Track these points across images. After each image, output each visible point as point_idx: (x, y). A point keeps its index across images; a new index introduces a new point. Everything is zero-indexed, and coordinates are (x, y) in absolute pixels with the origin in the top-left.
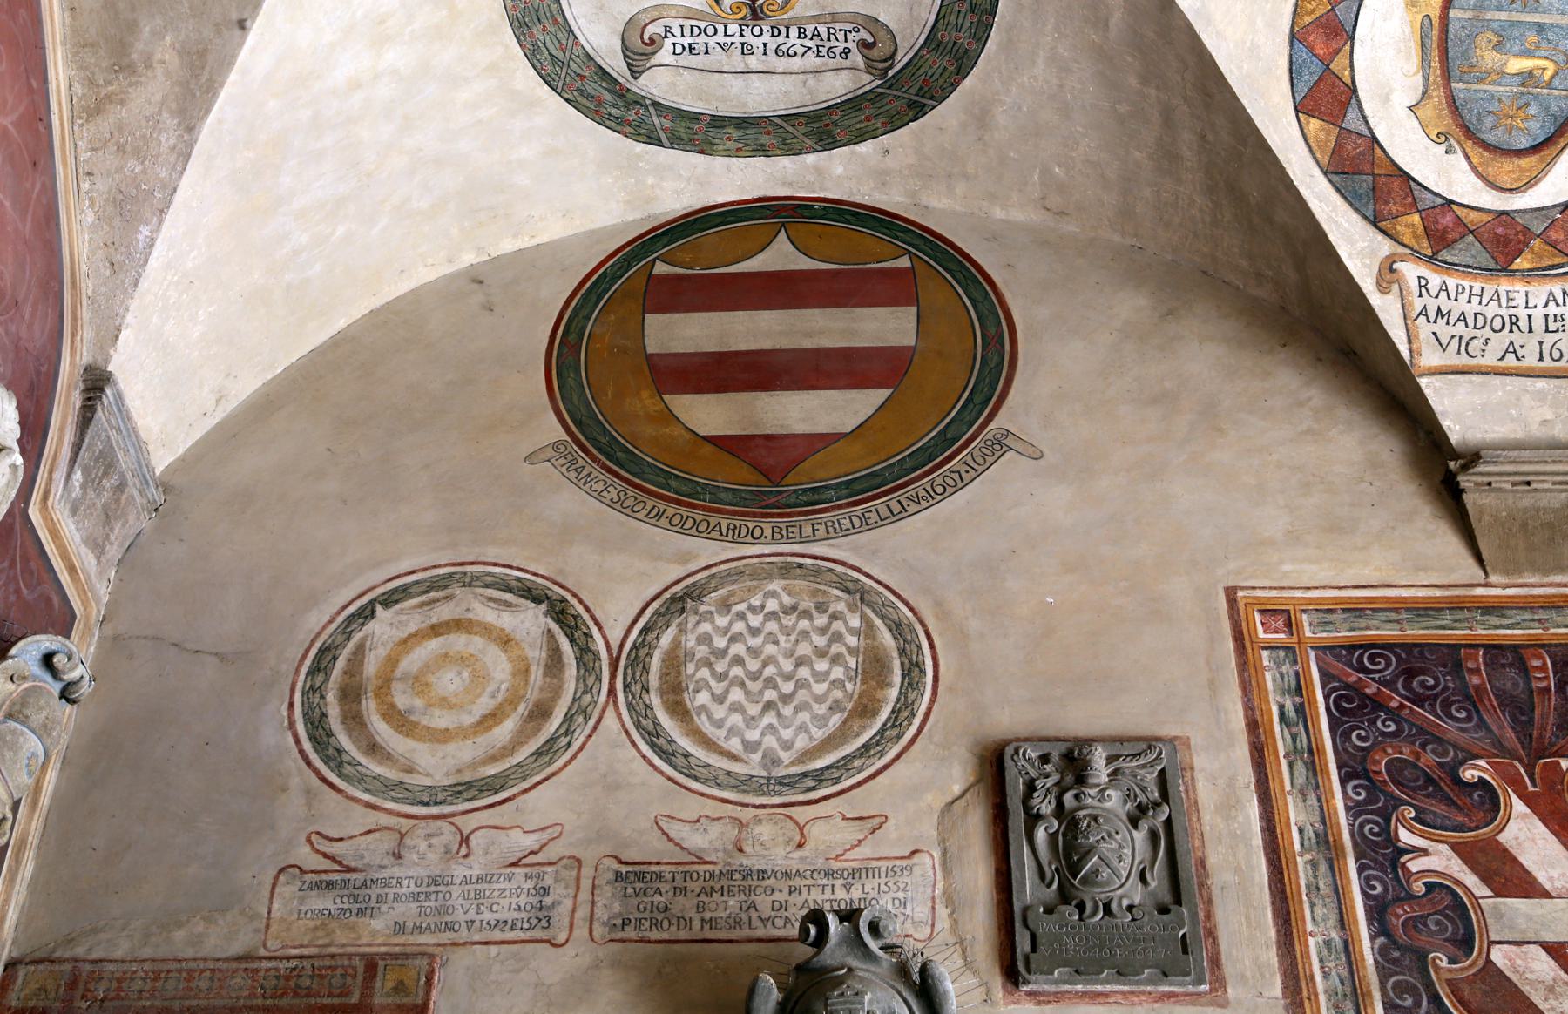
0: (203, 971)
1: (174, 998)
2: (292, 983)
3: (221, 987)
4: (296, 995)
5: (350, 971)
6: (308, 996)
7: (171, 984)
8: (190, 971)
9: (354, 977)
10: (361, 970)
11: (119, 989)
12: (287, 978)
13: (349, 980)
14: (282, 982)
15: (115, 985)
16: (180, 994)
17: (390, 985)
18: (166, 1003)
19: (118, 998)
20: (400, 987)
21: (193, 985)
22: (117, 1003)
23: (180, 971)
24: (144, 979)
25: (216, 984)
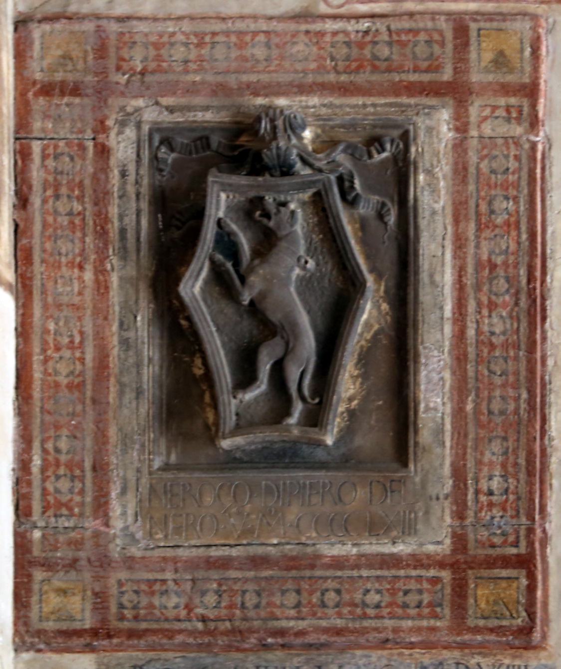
0: (255, 33)
1: (227, 72)
2: (367, 52)
3: (282, 57)
4: (375, 69)
5: (436, 37)
6: (389, 70)
7: (220, 52)
8: (240, 34)
9: (442, 44)
10: (449, 35)
11: (159, 58)
12: (361, 45)
13: (437, 49)
14: (355, 52)
15: (152, 52)
16: (234, 65)
17: (488, 56)
18: (220, 79)
19: (159, 70)
20: (500, 61)
21: (247, 52)
22: (157, 77)
23: (227, 33)
24: (186, 45)
25: (275, 52)
